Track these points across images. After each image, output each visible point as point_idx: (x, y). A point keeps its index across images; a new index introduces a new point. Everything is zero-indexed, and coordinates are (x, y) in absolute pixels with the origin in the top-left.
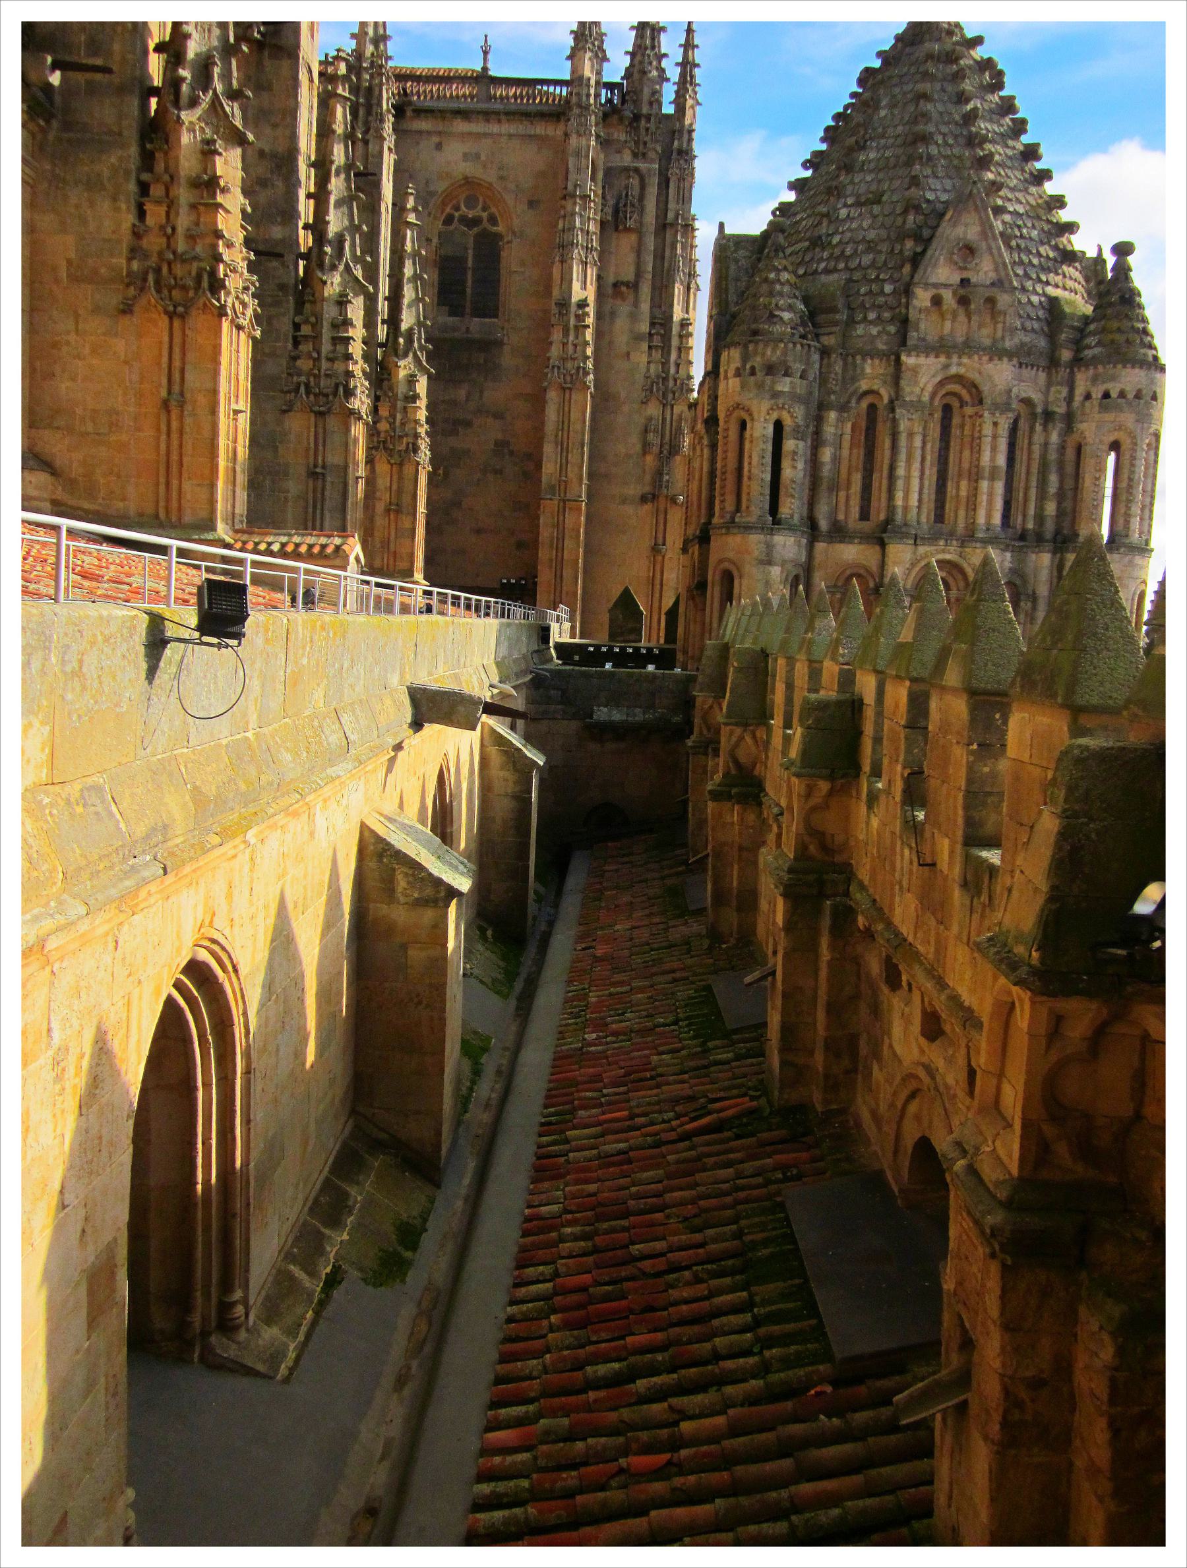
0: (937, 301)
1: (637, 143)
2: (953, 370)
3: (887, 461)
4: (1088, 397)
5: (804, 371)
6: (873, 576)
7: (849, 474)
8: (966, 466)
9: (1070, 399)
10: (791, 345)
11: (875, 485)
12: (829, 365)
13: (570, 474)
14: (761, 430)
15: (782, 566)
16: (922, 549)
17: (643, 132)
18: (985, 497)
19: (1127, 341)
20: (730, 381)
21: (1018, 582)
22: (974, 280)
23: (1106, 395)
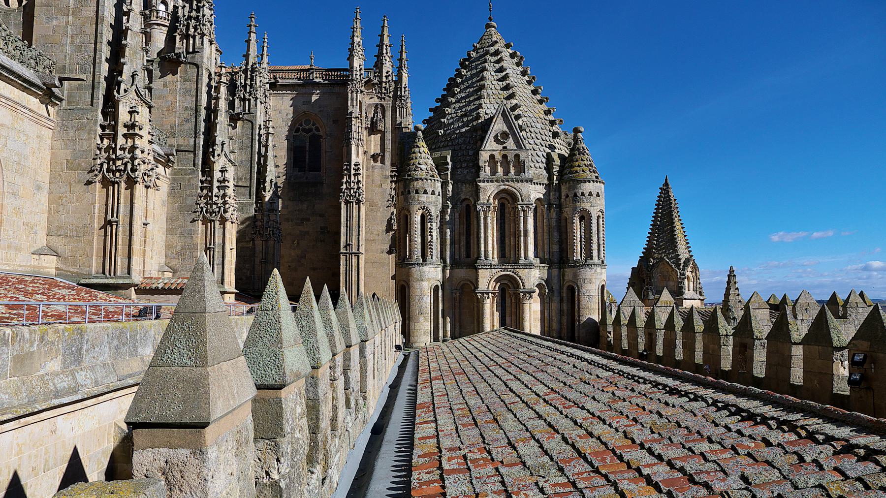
0: (492, 157)
1: (381, 93)
2: (503, 187)
4: (567, 196)
7: (460, 237)
9: (560, 198)
13: (354, 241)
16: (494, 271)
17: (384, 89)
19: (583, 171)
22: (508, 148)
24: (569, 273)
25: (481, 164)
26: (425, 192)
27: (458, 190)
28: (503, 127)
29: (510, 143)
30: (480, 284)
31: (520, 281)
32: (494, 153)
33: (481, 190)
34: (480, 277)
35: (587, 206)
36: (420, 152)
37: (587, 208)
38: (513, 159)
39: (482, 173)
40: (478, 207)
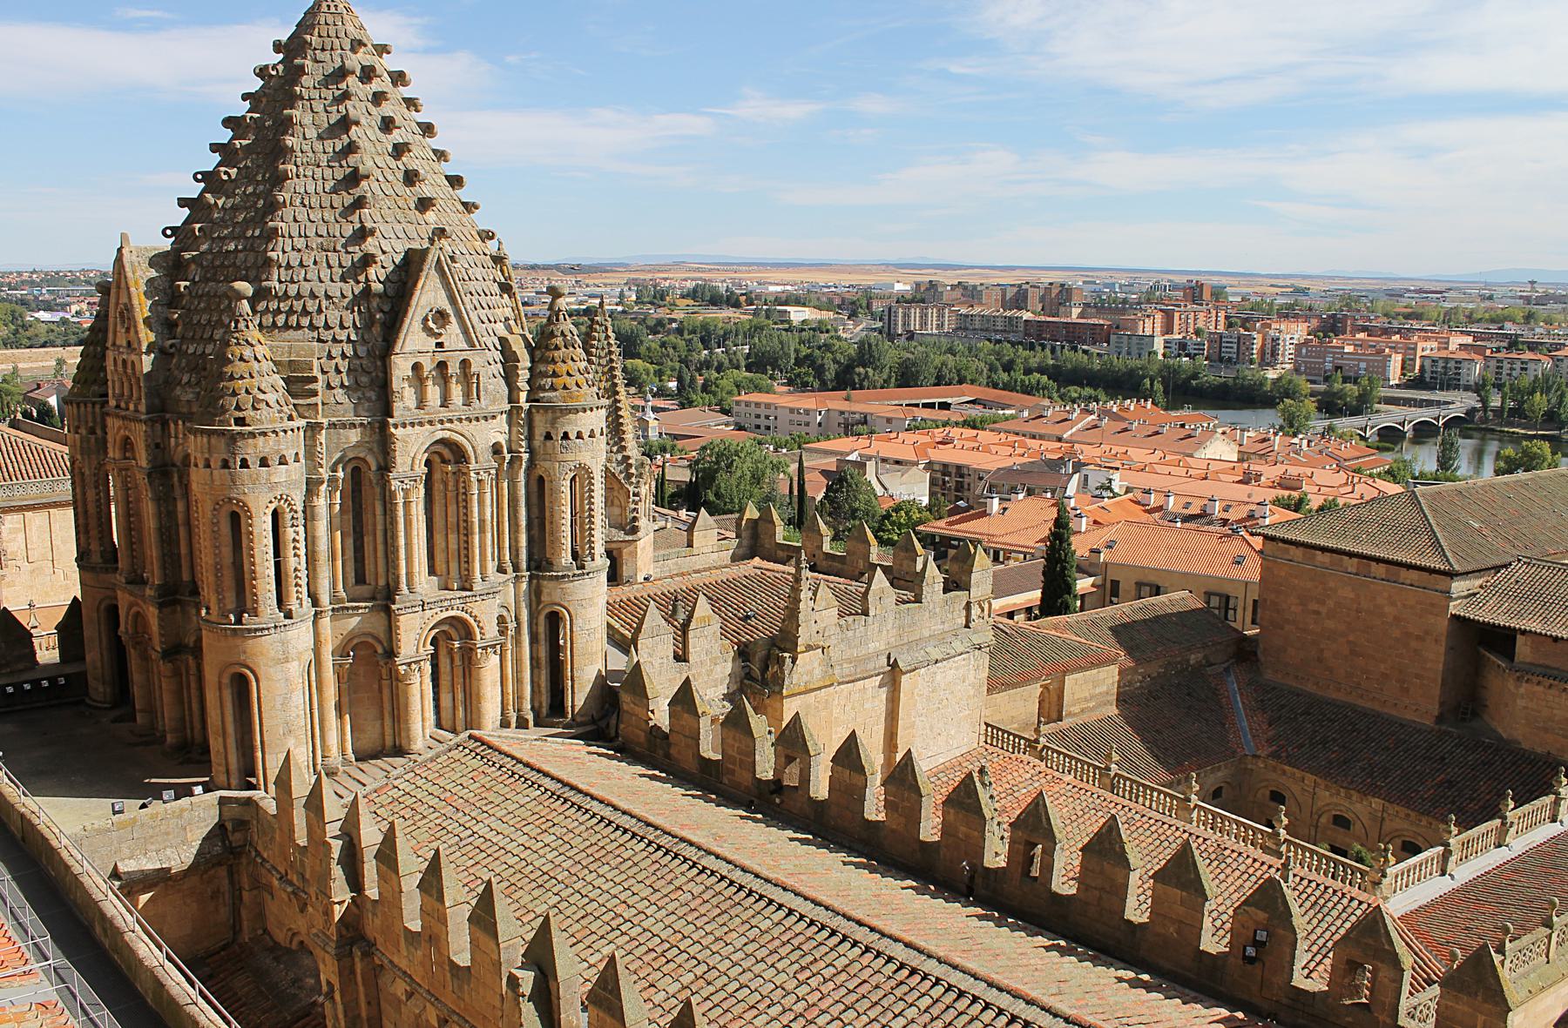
0: (417, 367)
2: (440, 435)
3: (380, 527)
4: (548, 437)
5: (297, 454)
6: (380, 642)
8: (452, 519)
10: (282, 434)
11: (368, 549)
12: (314, 438)
14: (262, 526)
15: (299, 660)
16: (428, 613)
18: (477, 551)
19: (577, 385)
20: (215, 472)
21: (505, 613)
23: (566, 436)
24: (550, 592)
25: (396, 384)
26: (283, 461)
27: (339, 439)
28: (435, 298)
29: (452, 335)
30: (402, 644)
31: (475, 625)
32: (421, 359)
33: (399, 445)
34: (401, 631)
35: (585, 458)
36: (256, 358)
37: (588, 464)
38: (458, 371)
39: (398, 407)
40: (393, 482)
